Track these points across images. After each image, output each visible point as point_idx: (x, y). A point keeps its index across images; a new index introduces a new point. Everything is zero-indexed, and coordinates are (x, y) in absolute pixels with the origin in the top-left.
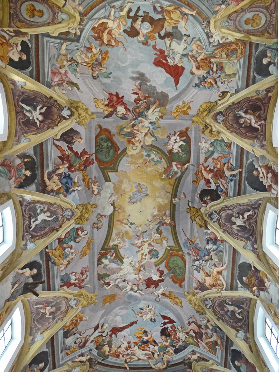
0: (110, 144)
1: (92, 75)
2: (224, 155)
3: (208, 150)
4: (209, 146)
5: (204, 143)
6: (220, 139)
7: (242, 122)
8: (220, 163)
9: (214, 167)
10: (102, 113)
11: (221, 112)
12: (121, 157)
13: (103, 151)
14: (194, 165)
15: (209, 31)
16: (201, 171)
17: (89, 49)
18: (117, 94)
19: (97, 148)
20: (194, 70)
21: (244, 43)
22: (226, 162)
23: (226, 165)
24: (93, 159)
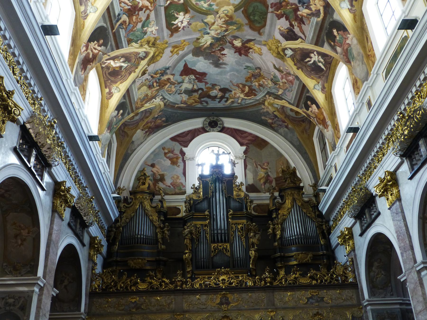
0: (252, 17)
1: (261, 70)
2: (132, 31)
3: (148, 26)
4: (148, 30)
5: (153, 31)
6: (139, 42)
7: (122, 59)
8: (134, 21)
9: (138, 14)
10: (256, 44)
11: (143, 59)
12: (241, 4)
13: (260, 13)
14: (160, 7)
15: (164, 101)
16: (151, 4)
17: (260, 85)
18: (240, 54)
19: (265, 16)
20: (171, 77)
21: (137, 108)
22: (129, 27)
23: (127, 24)
24: (272, 7)
